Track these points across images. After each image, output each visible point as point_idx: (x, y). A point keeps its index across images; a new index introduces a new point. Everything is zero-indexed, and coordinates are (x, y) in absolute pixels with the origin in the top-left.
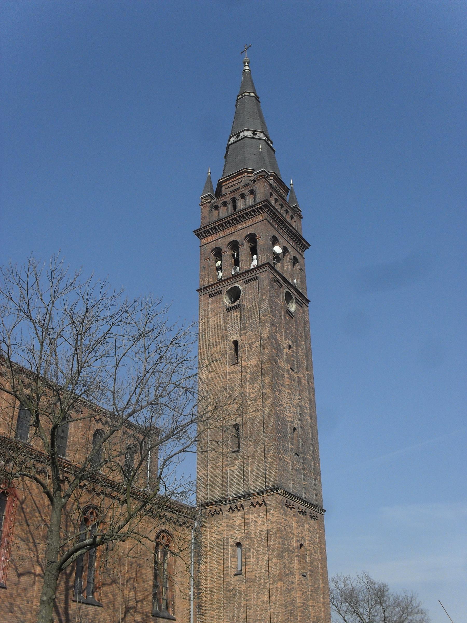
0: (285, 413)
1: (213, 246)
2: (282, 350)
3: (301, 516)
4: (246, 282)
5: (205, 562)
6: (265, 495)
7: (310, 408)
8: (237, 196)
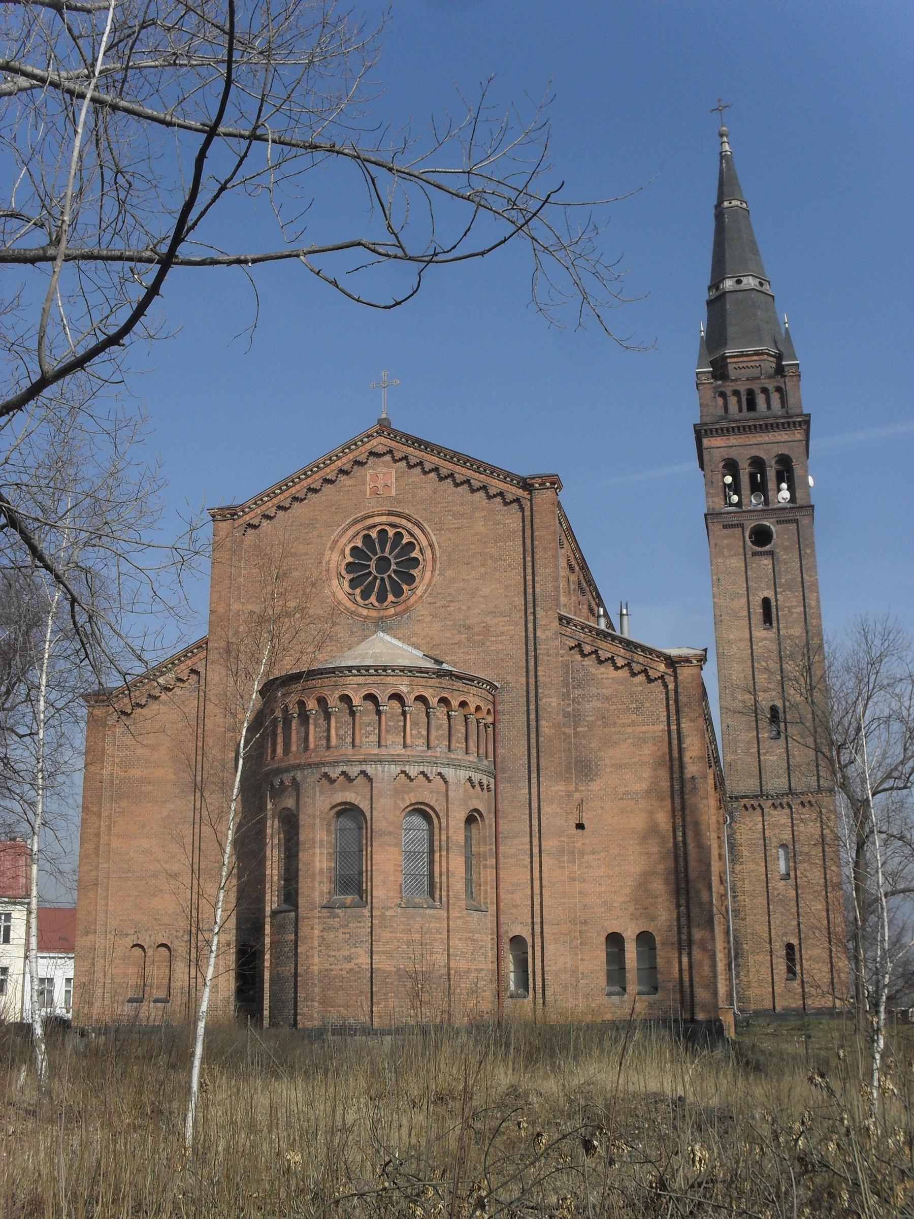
1: (725, 453)
4: (778, 522)
8: (756, 387)
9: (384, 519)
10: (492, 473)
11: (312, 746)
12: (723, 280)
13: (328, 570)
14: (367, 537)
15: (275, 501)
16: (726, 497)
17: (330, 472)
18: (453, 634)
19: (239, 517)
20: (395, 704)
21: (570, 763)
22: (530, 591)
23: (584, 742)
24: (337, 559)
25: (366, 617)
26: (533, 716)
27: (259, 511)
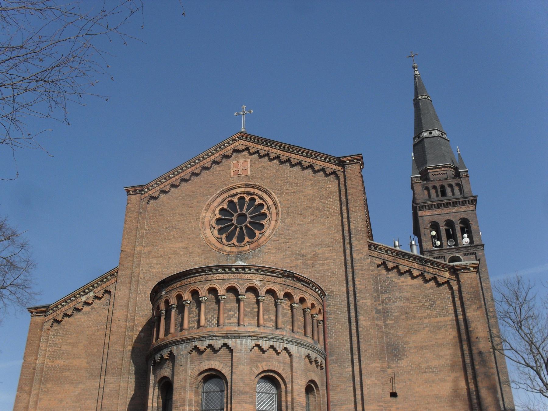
1: (431, 219)
4: (465, 255)
8: (445, 184)
9: (242, 190)
10: (316, 157)
11: (186, 326)
12: (421, 133)
13: (203, 223)
14: (231, 203)
15: (169, 182)
16: (434, 243)
17: (207, 163)
18: (291, 261)
19: (146, 192)
20: (251, 296)
21: (383, 346)
22: (346, 228)
23: (392, 331)
24: (209, 216)
25: (230, 252)
26: (353, 314)
27: (158, 188)
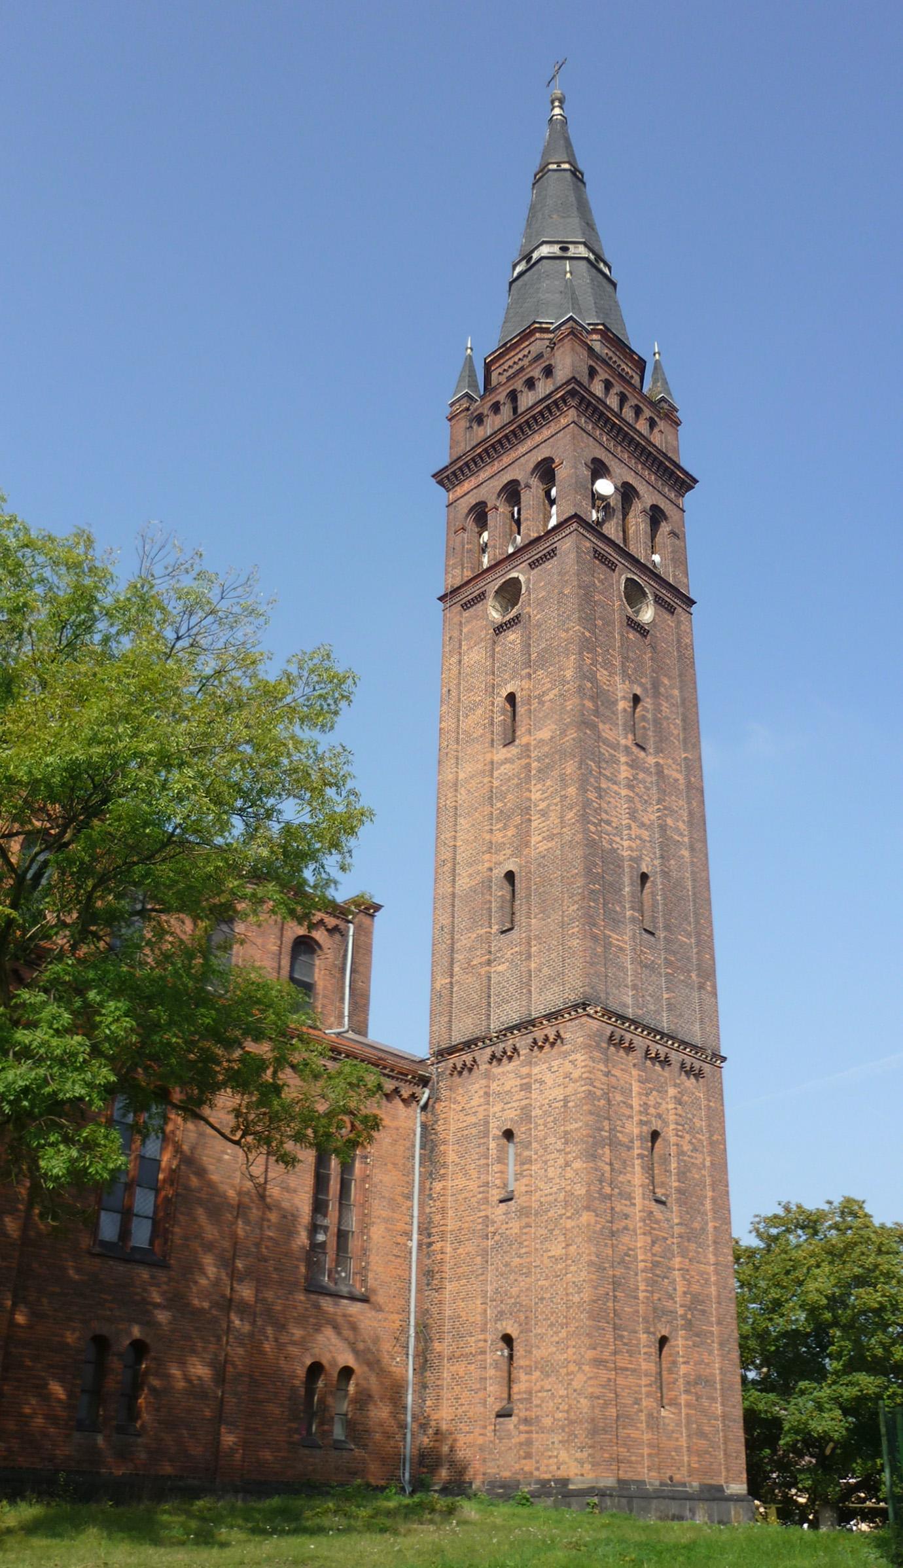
0: (618, 839)
1: (472, 500)
2: (615, 703)
3: (658, 1067)
4: (532, 566)
5: (443, 1176)
6: (560, 1019)
7: (690, 832)
8: (518, 384)
